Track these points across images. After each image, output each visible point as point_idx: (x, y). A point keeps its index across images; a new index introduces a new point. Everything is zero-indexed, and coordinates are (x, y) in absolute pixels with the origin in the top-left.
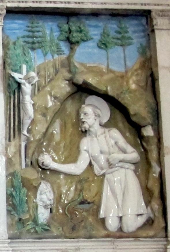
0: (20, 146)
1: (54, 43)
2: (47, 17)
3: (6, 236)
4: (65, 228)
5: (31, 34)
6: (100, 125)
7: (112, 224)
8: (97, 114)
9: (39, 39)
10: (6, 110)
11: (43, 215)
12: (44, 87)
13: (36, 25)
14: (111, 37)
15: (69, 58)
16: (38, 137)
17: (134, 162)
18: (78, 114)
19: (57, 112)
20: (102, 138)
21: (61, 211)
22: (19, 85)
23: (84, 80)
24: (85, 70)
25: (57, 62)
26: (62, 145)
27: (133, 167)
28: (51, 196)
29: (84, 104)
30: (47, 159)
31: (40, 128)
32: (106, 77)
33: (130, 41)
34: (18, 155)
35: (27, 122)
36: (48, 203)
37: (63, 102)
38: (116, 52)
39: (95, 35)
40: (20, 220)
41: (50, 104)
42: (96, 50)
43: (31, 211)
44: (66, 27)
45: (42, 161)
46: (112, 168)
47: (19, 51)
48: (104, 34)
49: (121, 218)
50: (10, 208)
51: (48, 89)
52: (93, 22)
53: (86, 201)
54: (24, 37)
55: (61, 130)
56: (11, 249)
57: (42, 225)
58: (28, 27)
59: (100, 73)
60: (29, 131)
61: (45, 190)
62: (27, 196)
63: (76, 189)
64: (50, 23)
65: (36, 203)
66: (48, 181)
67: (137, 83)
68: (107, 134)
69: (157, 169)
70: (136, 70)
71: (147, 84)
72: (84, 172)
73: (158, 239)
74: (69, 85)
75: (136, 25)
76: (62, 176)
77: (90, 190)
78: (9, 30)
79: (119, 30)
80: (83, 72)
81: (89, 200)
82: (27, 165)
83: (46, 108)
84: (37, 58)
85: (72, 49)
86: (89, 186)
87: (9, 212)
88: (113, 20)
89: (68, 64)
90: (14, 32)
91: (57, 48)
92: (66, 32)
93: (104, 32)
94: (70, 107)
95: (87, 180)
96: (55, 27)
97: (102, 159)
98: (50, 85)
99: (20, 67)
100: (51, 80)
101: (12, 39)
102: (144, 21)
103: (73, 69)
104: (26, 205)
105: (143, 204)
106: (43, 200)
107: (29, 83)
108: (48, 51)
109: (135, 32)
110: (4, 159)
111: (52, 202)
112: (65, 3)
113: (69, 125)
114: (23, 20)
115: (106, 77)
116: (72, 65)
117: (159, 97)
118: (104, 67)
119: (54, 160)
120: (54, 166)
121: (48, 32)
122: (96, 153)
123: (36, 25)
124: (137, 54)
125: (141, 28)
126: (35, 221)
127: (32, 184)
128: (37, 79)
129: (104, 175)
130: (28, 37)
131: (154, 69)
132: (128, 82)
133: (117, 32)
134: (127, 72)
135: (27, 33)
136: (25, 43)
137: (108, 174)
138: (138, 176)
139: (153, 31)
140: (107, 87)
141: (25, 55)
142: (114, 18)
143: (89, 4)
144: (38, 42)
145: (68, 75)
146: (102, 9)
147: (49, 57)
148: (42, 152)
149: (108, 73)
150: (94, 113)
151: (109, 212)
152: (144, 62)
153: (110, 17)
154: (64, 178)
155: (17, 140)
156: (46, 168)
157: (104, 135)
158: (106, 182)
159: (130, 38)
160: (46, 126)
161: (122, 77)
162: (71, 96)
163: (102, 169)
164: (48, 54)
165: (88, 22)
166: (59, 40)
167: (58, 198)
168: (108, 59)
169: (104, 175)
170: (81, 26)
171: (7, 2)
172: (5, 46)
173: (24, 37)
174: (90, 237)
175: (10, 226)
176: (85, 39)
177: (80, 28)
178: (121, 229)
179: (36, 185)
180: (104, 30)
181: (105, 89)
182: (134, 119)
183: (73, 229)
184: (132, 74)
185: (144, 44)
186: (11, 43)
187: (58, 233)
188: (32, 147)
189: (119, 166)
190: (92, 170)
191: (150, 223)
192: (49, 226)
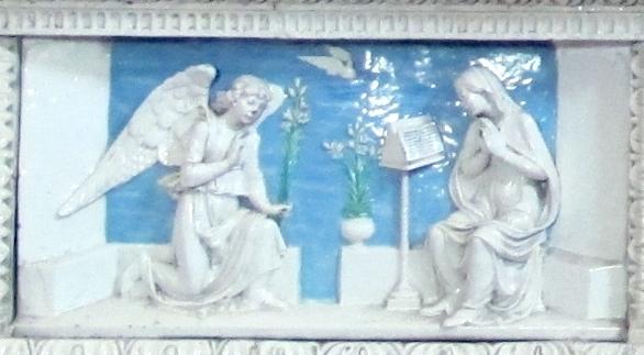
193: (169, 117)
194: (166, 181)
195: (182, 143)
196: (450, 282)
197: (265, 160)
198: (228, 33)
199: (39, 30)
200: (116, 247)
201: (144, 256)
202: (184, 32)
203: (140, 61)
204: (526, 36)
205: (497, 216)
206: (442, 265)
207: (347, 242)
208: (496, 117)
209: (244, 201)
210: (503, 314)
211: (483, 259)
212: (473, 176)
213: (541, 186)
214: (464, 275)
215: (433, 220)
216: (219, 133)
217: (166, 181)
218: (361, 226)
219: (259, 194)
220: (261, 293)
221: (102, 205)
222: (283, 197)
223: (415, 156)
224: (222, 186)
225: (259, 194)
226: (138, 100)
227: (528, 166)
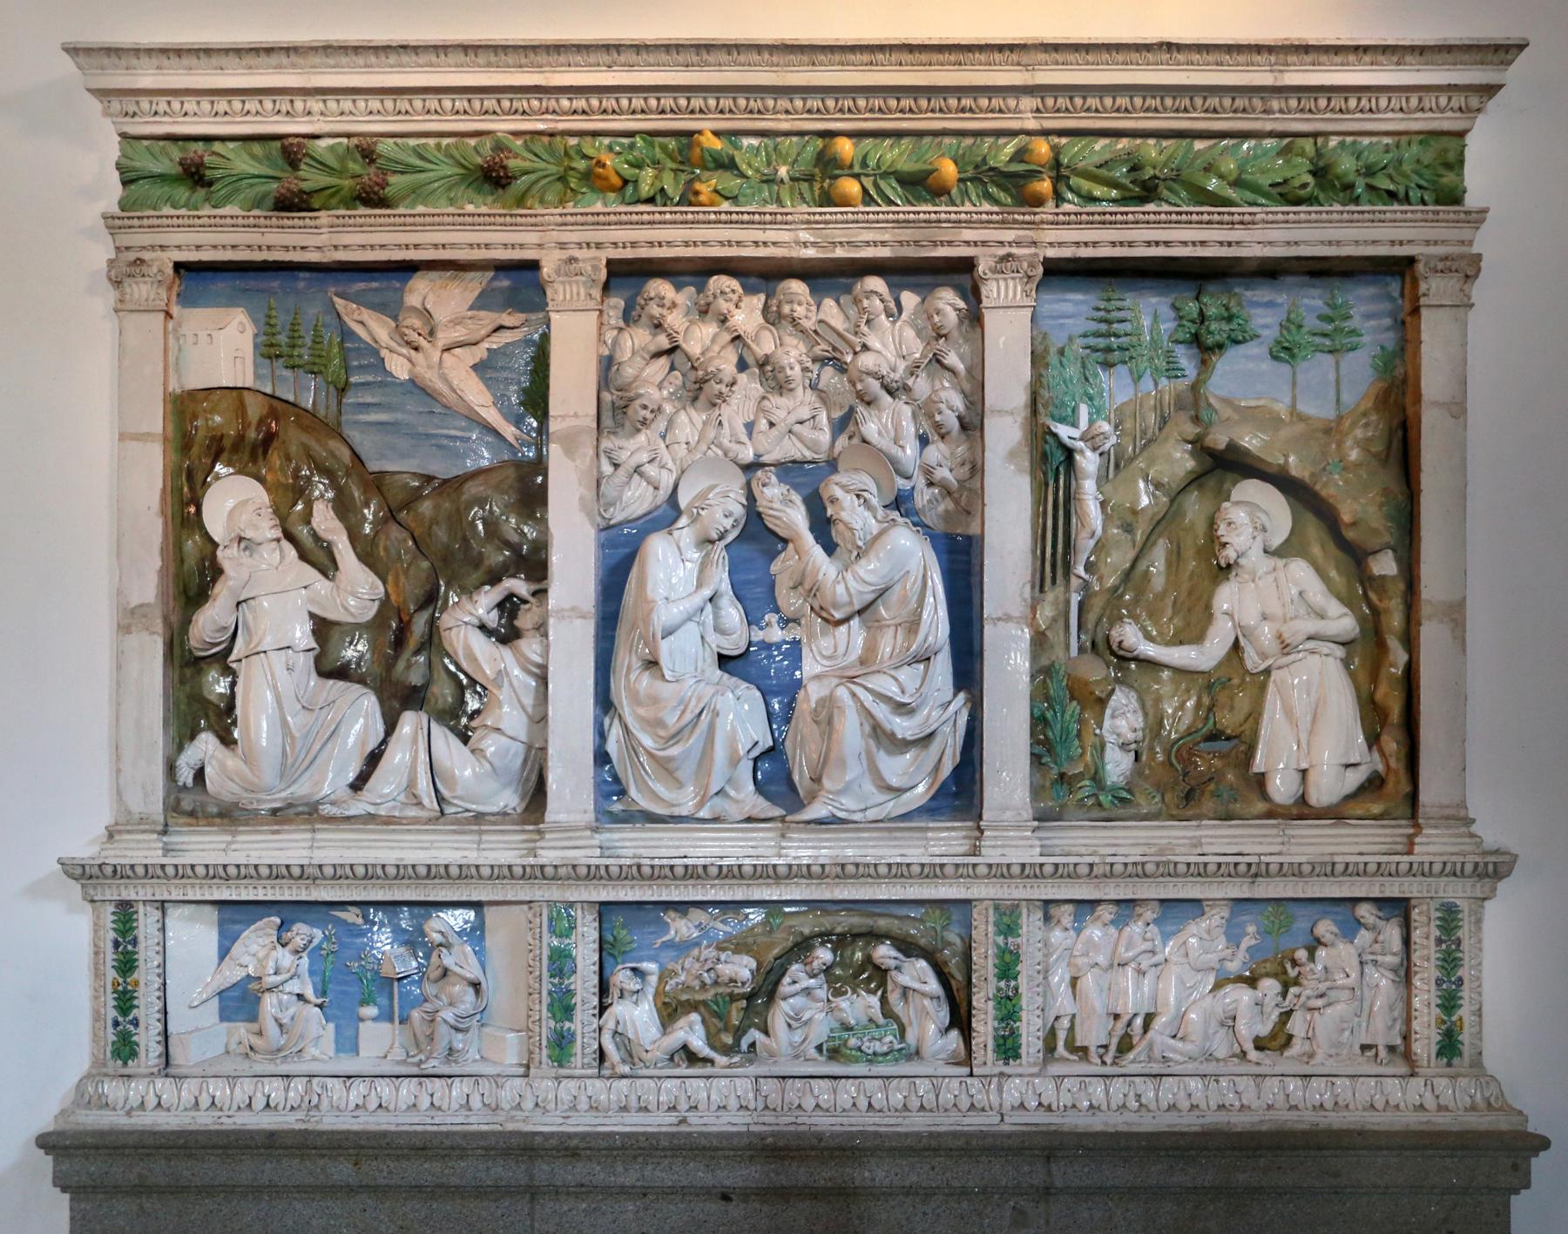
0: (1068, 602)
2: (1148, 283)
3: (1028, 813)
4: (1168, 797)
5: (1103, 327)
6: (1266, 551)
7: (1281, 788)
10: (1035, 515)
11: (1117, 766)
12: (1132, 459)
13: (1119, 304)
14: (1305, 330)
15: (1195, 388)
16: (1111, 581)
18: (1212, 524)
19: (1159, 522)
21: (1160, 757)
22: (1069, 453)
24: (1236, 417)
26: (1169, 601)
27: (1340, 652)
28: (1138, 721)
29: (1228, 499)
30: (1130, 635)
31: (1119, 559)
32: (1285, 433)
33: (1355, 339)
34: (1061, 623)
35: (1085, 546)
36: (1130, 736)
37: (1177, 495)
38: (1317, 368)
39: (1266, 326)
40: (1062, 776)
41: (1145, 501)
42: (1267, 365)
43: (1088, 758)
44: (1192, 308)
47: (1072, 371)
48: (1290, 324)
49: (1304, 772)
50: (1039, 749)
51: (1141, 463)
52: (1262, 293)
53: (1222, 733)
54: (1085, 336)
55: (1169, 564)
56: (1038, 843)
57: (1114, 789)
58: (1098, 309)
59: (1275, 422)
60: (1089, 567)
62: (1080, 721)
63: (1198, 705)
64: (1154, 300)
65: (1101, 737)
66: (1131, 687)
67: (1364, 445)
68: (1281, 574)
69: (1399, 656)
70: (1365, 414)
71: (1389, 448)
72: (1220, 665)
73: (1393, 822)
74: (1192, 454)
75: (1374, 299)
76: (1166, 674)
77: (1232, 708)
78: (1053, 318)
81: (1229, 731)
82: (1081, 650)
83: (1134, 512)
84: (1116, 387)
85: (1204, 362)
86: (1232, 698)
87: (1036, 759)
88: (1314, 286)
89: (1194, 403)
92: (1193, 322)
93: (1288, 320)
94: (1194, 507)
95: (1225, 684)
96: (1165, 310)
97: (1266, 632)
98: (1145, 454)
99: (1075, 410)
100: (1150, 441)
101: (1057, 340)
102: (1394, 287)
103: (1204, 415)
104: (1076, 743)
105: (1361, 739)
107: (1094, 449)
109: (1368, 316)
110: (1027, 633)
111: (1140, 734)
112: (1194, 243)
113: (1189, 553)
114: (1086, 292)
115: (1285, 433)
116: (1203, 404)
117: (1419, 483)
118: (1282, 408)
119: (1149, 637)
120: (1149, 650)
121: (1146, 322)
122: (1250, 617)
123: (1119, 304)
124: (1370, 371)
125: (1386, 306)
126: (1097, 778)
127: (1092, 693)
128: (1113, 440)
129: (1267, 672)
130: (1097, 335)
131: (1410, 410)
132: (1340, 444)
133: (1322, 318)
134: (1340, 418)
135: (1094, 326)
138: (1352, 675)
139: (1416, 311)
140: (1286, 456)
142: (1316, 281)
144: (1120, 348)
145: (1191, 430)
146: (1287, 259)
147: (1147, 384)
148: (1121, 618)
149: (1292, 422)
151: (1278, 760)
153: (1307, 278)
154: (1172, 680)
155: (1060, 589)
156: (1129, 655)
157: (1271, 578)
158: (1271, 688)
159: (1353, 332)
160: (1131, 555)
161: (1328, 431)
162: (1195, 480)
163: (1264, 656)
165: (1249, 294)
167: (1155, 727)
168: (1294, 384)
169: (1267, 672)
172: (1038, 359)
173: (1085, 336)
174: (1228, 817)
175: (1036, 792)
177: (1227, 309)
178: (1302, 800)
179: (1103, 696)
181: (1282, 462)
182: (1350, 534)
183: (1189, 797)
184: (1354, 425)
186: (1053, 350)
187: (1154, 809)
188: (1097, 605)
190: (1241, 660)
191: (1374, 784)
192: (1129, 791)
193: (254, 948)
194: (253, 986)
195: (261, 963)
196: (423, 1041)
197: (311, 973)
198: (287, 897)
199: (173, 897)
200: (226, 1024)
201: (242, 1030)
202: (261, 898)
203: (234, 915)
204: (464, 898)
205: (451, 1004)
206: (418, 1032)
207: (362, 1020)
208: (448, 946)
209: (300, 997)
210: (456, 1062)
211: (443, 1030)
212: (436, 981)
213: (476, 986)
214: (431, 1038)
215: (413, 1008)
216: (285, 957)
217: (253, 986)
218: (371, 1011)
219: (309, 993)
220: (313, 1051)
221: (216, 999)
222: (324, 994)
223: (400, 969)
224: (288, 987)
225: (309, 993)
226: (235, 939)
227: (468, 975)
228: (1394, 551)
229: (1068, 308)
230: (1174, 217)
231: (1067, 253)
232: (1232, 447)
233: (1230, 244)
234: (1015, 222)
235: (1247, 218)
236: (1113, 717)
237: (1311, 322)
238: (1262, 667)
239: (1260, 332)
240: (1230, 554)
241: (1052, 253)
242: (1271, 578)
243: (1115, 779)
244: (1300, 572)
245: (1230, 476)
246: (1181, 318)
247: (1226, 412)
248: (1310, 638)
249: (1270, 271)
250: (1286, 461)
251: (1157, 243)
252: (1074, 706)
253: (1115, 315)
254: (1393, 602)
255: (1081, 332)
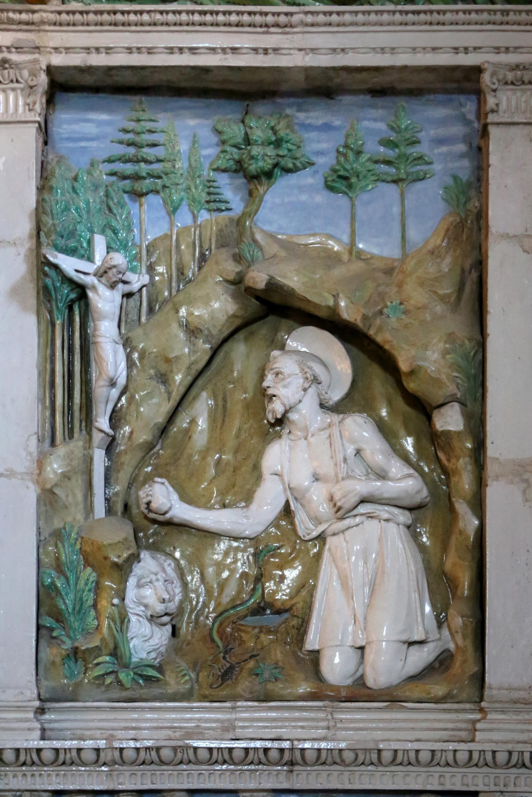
1: (199, 177)
2: (185, 101)
5: (132, 151)
7: (337, 666)
8: (308, 375)
9: (157, 167)
11: (145, 641)
13: (149, 125)
14: (364, 158)
17: (407, 503)
20: (319, 441)
23: (271, 278)
24: (283, 253)
25: (207, 234)
30: (162, 496)
34: (78, 482)
36: (160, 608)
38: (380, 200)
42: (322, 197)
44: (236, 132)
45: (145, 501)
46: (342, 518)
47: (94, 199)
52: (316, 115)
54: (110, 161)
61: (153, 577)
64: (192, 122)
75: (443, 122)
79: (393, 136)
80: (274, 256)
84: (150, 221)
85: (251, 194)
88: (373, 106)
90: (85, 148)
91: (209, 194)
96: (206, 134)
99: (90, 242)
106: (145, 601)
108: (182, 200)
110: (31, 494)
112: (224, 50)
114: (109, 110)
115: (338, 272)
120: (182, 512)
121: (183, 147)
122: (302, 478)
136: (114, 178)
137: (334, 534)
140: (336, 297)
141: (110, 210)
142: (379, 101)
143: (297, 52)
144: (150, 175)
150: (304, 369)
152: (461, 225)
155: (77, 444)
161: (389, 271)
164: (179, 211)
165: (301, 116)
166: (214, 170)
170: (281, 127)
171: (53, 51)
173: (110, 161)
176: (290, 165)
180: (347, 136)
181: (331, 303)
182: (411, 386)
185: (465, 175)
187: (184, 688)
189: (362, 515)
191: (442, 663)
228: (463, 404)
229: (90, 129)
230: (197, 18)
231: (76, 60)
232: (273, 286)
233: (266, 51)
234: (11, 21)
235: (283, 19)
236: (139, 586)
237: (374, 148)
238: (315, 534)
239: (314, 159)
240: (277, 408)
241: (57, 60)
242: (324, 435)
243: (144, 655)
244: (359, 429)
245: (285, 323)
246: (224, 142)
247: (272, 249)
248: (363, 501)
249: (323, 87)
250: (337, 304)
251: (181, 50)
252: (88, 574)
253: (147, 138)
254: (461, 461)
255: (105, 156)
